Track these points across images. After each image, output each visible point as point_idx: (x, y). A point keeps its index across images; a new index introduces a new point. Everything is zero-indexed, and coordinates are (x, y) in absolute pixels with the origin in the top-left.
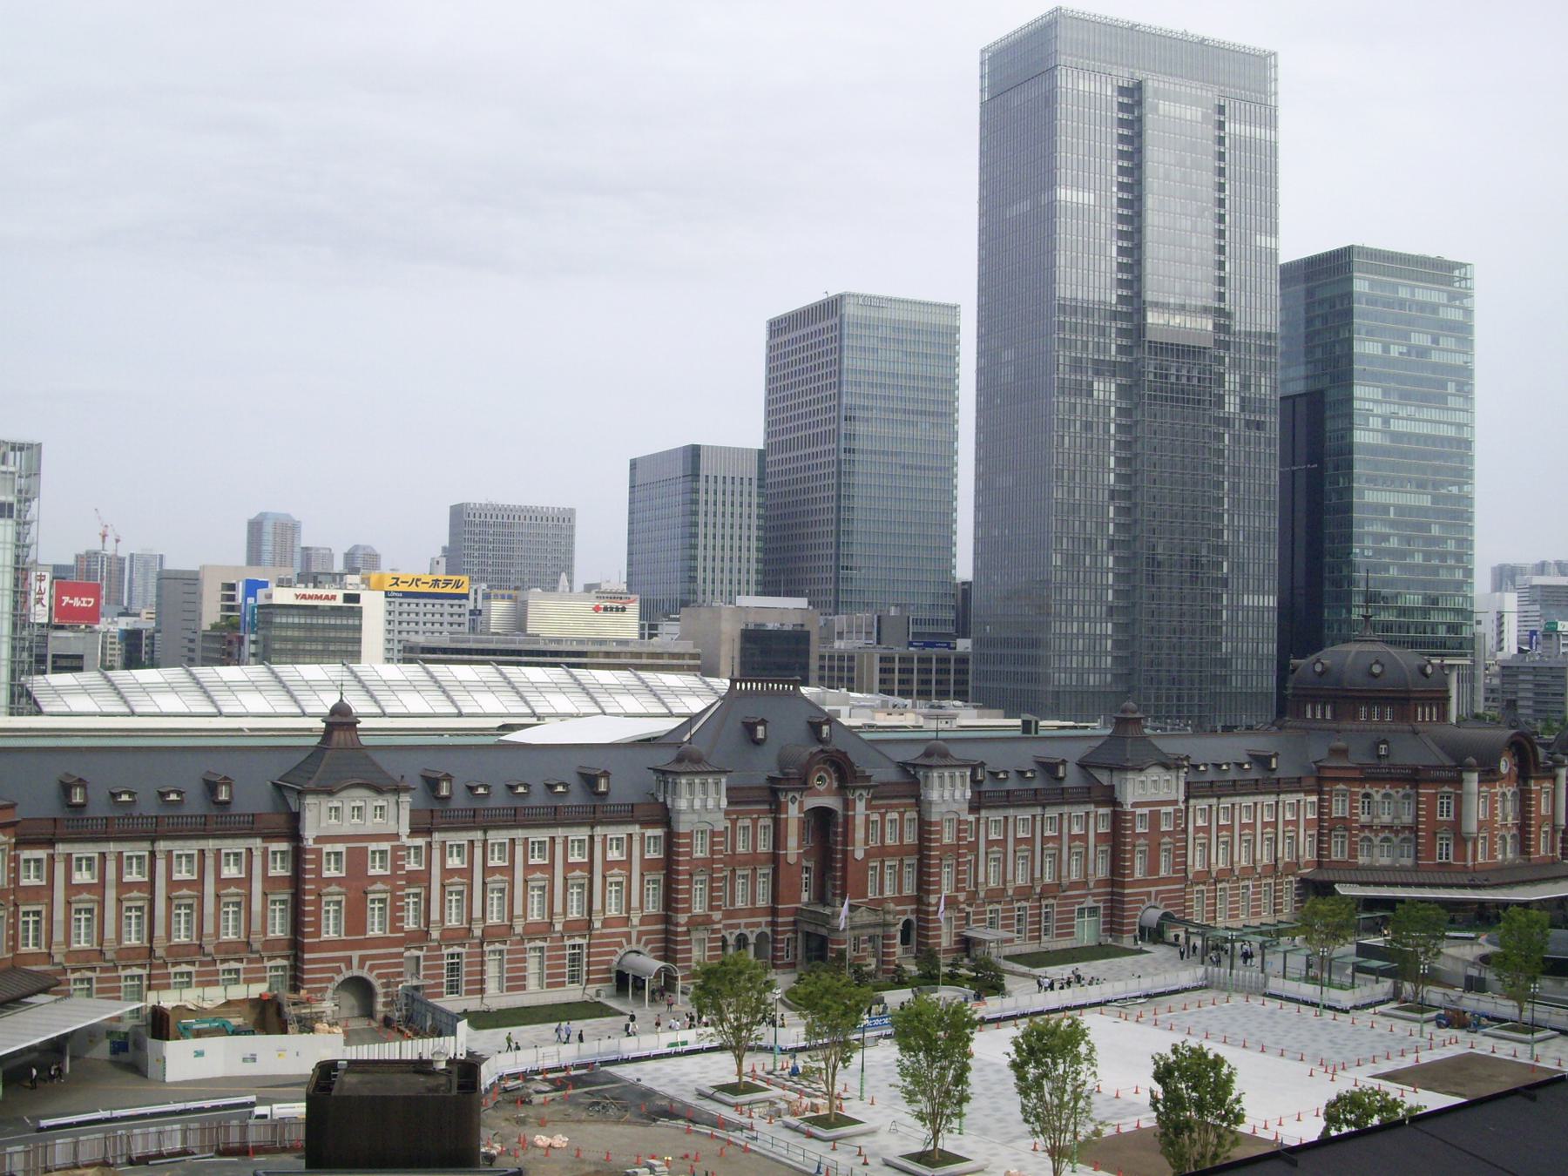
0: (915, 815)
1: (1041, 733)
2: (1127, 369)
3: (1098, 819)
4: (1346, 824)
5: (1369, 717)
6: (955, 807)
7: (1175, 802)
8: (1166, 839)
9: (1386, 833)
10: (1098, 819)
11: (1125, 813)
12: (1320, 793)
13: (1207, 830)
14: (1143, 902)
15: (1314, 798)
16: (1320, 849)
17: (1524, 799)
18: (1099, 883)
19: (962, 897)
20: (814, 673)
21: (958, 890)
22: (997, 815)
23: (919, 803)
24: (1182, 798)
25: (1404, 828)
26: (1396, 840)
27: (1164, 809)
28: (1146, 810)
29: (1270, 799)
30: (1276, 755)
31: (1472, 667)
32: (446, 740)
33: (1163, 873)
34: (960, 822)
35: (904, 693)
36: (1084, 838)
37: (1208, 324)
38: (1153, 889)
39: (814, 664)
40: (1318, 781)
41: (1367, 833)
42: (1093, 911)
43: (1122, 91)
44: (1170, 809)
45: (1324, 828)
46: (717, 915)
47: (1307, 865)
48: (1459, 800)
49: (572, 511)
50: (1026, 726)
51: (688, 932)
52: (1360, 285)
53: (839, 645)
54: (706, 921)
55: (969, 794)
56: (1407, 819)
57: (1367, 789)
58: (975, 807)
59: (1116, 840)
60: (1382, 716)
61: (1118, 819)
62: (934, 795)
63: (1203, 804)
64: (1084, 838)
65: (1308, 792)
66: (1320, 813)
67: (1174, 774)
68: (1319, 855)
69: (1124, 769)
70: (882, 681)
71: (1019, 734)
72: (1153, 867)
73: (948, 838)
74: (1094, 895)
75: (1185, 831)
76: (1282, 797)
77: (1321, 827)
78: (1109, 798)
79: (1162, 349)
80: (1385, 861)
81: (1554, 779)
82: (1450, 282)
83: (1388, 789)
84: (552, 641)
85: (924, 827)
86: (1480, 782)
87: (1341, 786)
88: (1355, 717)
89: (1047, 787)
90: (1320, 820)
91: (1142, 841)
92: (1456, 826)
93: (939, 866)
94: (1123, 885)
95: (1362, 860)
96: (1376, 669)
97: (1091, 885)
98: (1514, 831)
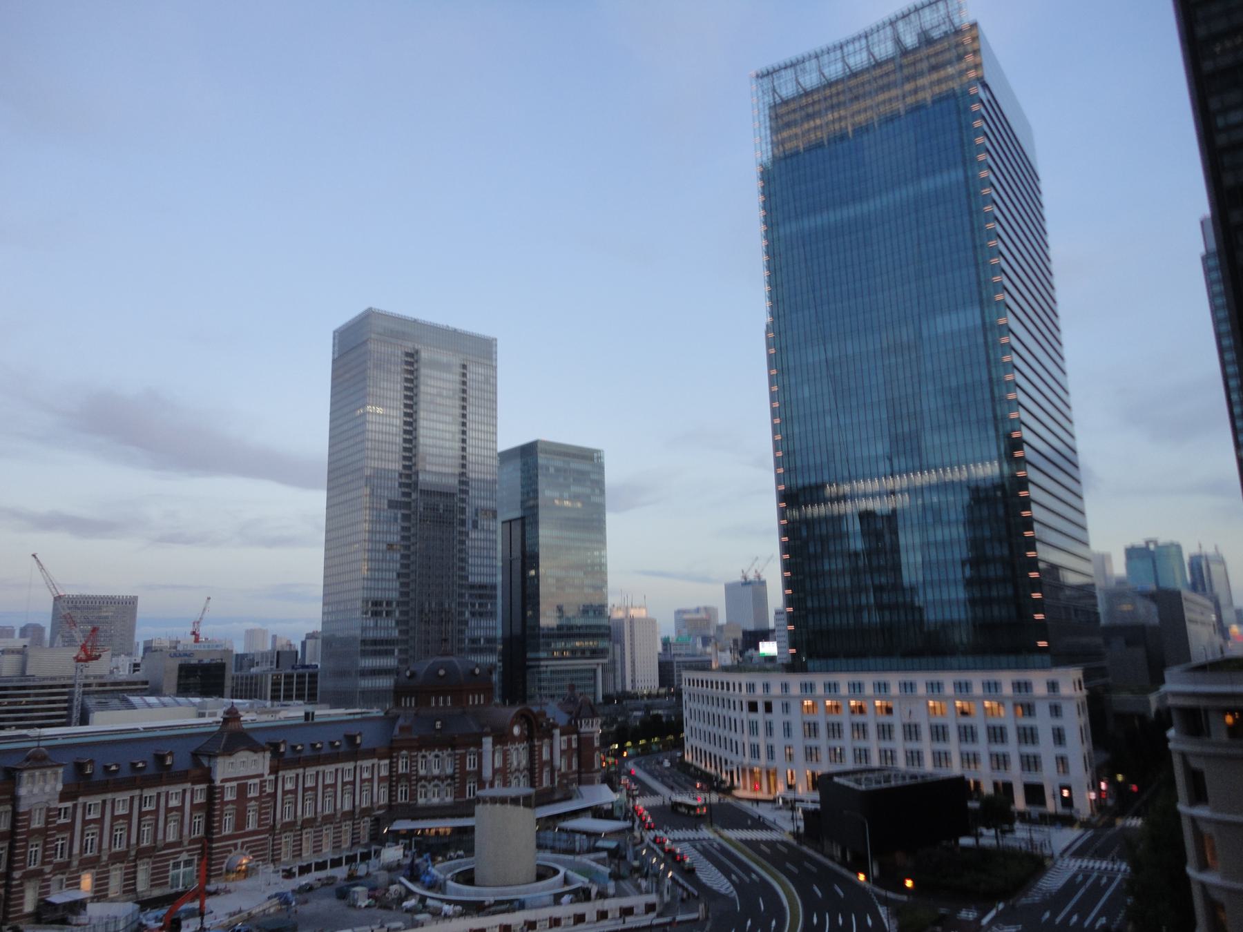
0: (9, 808)
1: (316, 720)
2: (407, 505)
3: (199, 793)
4: (407, 777)
5: (437, 702)
6: (46, 798)
7: (262, 775)
8: (253, 803)
9: (436, 782)
10: (199, 793)
11: (216, 787)
12: (391, 757)
13: (295, 792)
14: (230, 852)
15: (387, 762)
16: (390, 796)
17: (532, 753)
18: (192, 842)
19: (48, 869)
20: (227, 690)
21: (43, 863)
22: (96, 800)
23: (14, 800)
24: (267, 771)
25: (447, 777)
26: (442, 786)
27: (250, 782)
28: (234, 784)
29: (349, 766)
30: (360, 734)
31: (614, 662)
32: (60, 742)
33: (252, 826)
34: (49, 810)
35: (288, 697)
36: (181, 809)
37: (454, 482)
38: (240, 841)
39: (228, 683)
40: (390, 751)
41: (423, 782)
42: (188, 863)
43: (407, 354)
44: (257, 781)
45: (393, 780)
46: (48, 869)
47: (380, 808)
48: (480, 756)
49: (136, 598)
50: (307, 715)
51: (21, 885)
52: (542, 460)
53: (253, 670)
54: (39, 873)
55: (60, 787)
56: (449, 771)
57: (423, 752)
58: (64, 797)
59: (210, 808)
60: (445, 701)
61: (211, 792)
62: (23, 791)
63: (291, 774)
64: (181, 809)
65: (380, 758)
66: (391, 771)
67: (261, 754)
68: (390, 800)
69: (216, 756)
70: (272, 690)
71: (302, 721)
72: (241, 821)
73: (36, 824)
74: (188, 851)
75: (274, 795)
76: (359, 763)
77: (391, 781)
78: (207, 777)
79: (426, 493)
80: (436, 801)
81: (551, 737)
82: (592, 459)
83: (437, 752)
84: (44, 679)
85: (15, 814)
86: (494, 744)
87: (404, 752)
88: (429, 703)
89: (161, 773)
90: (391, 776)
91: (230, 806)
92: (479, 772)
93: (26, 847)
94: (211, 841)
95: (421, 801)
96: (442, 672)
97: (186, 843)
98: (526, 772)
